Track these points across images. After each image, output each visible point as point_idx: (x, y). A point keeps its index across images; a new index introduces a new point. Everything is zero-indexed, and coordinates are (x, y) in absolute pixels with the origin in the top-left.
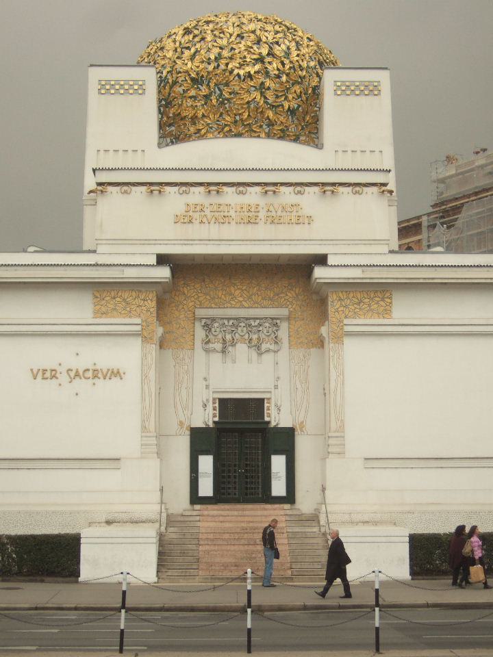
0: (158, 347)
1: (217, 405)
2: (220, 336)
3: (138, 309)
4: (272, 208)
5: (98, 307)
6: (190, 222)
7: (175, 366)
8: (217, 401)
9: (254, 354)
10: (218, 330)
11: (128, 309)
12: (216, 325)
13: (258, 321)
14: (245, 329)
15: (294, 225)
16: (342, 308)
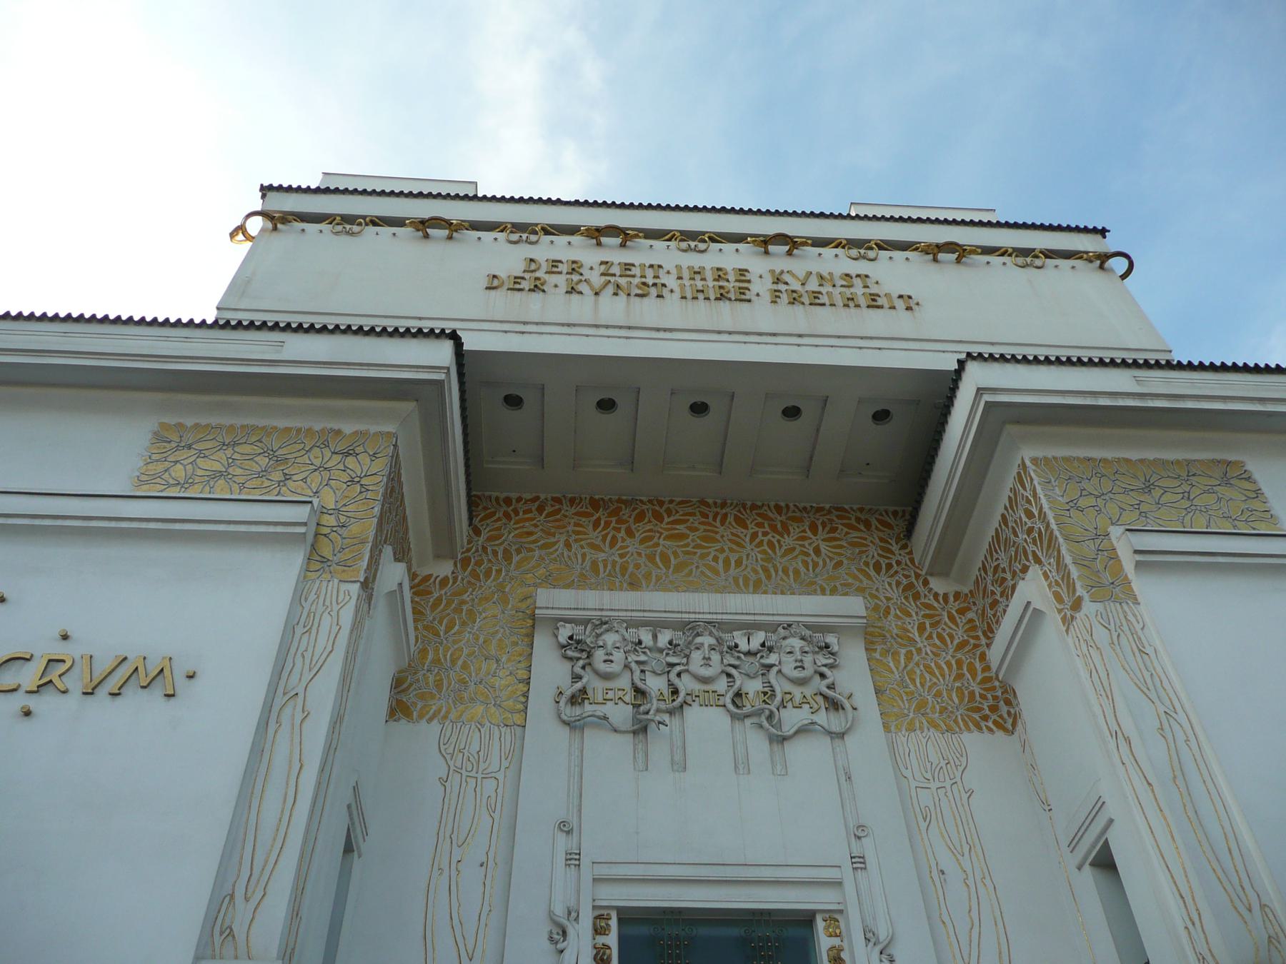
0: (378, 693)
1: (612, 939)
2: (624, 682)
3: (315, 479)
4: (786, 277)
5: (160, 467)
6: (536, 288)
7: (443, 782)
8: (614, 923)
9: (757, 743)
10: (618, 656)
11: (277, 476)
12: (610, 639)
13: (758, 638)
14: (715, 657)
15: (865, 311)
16: (1092, 501)
